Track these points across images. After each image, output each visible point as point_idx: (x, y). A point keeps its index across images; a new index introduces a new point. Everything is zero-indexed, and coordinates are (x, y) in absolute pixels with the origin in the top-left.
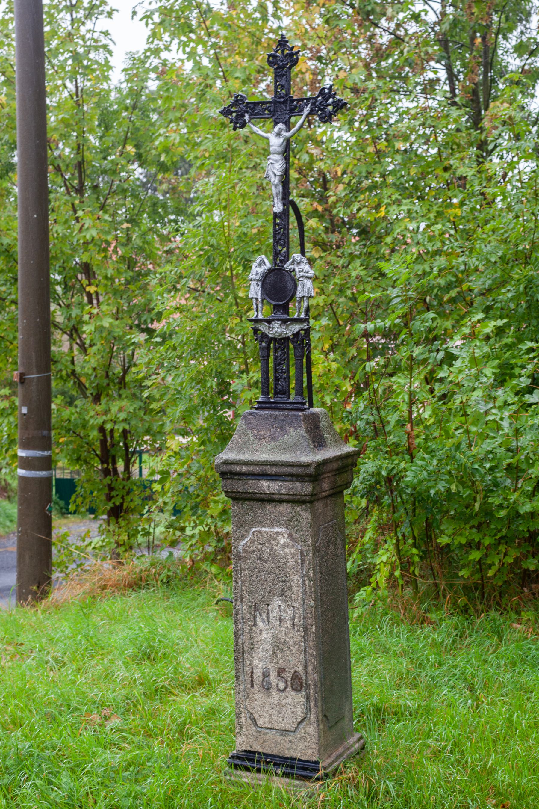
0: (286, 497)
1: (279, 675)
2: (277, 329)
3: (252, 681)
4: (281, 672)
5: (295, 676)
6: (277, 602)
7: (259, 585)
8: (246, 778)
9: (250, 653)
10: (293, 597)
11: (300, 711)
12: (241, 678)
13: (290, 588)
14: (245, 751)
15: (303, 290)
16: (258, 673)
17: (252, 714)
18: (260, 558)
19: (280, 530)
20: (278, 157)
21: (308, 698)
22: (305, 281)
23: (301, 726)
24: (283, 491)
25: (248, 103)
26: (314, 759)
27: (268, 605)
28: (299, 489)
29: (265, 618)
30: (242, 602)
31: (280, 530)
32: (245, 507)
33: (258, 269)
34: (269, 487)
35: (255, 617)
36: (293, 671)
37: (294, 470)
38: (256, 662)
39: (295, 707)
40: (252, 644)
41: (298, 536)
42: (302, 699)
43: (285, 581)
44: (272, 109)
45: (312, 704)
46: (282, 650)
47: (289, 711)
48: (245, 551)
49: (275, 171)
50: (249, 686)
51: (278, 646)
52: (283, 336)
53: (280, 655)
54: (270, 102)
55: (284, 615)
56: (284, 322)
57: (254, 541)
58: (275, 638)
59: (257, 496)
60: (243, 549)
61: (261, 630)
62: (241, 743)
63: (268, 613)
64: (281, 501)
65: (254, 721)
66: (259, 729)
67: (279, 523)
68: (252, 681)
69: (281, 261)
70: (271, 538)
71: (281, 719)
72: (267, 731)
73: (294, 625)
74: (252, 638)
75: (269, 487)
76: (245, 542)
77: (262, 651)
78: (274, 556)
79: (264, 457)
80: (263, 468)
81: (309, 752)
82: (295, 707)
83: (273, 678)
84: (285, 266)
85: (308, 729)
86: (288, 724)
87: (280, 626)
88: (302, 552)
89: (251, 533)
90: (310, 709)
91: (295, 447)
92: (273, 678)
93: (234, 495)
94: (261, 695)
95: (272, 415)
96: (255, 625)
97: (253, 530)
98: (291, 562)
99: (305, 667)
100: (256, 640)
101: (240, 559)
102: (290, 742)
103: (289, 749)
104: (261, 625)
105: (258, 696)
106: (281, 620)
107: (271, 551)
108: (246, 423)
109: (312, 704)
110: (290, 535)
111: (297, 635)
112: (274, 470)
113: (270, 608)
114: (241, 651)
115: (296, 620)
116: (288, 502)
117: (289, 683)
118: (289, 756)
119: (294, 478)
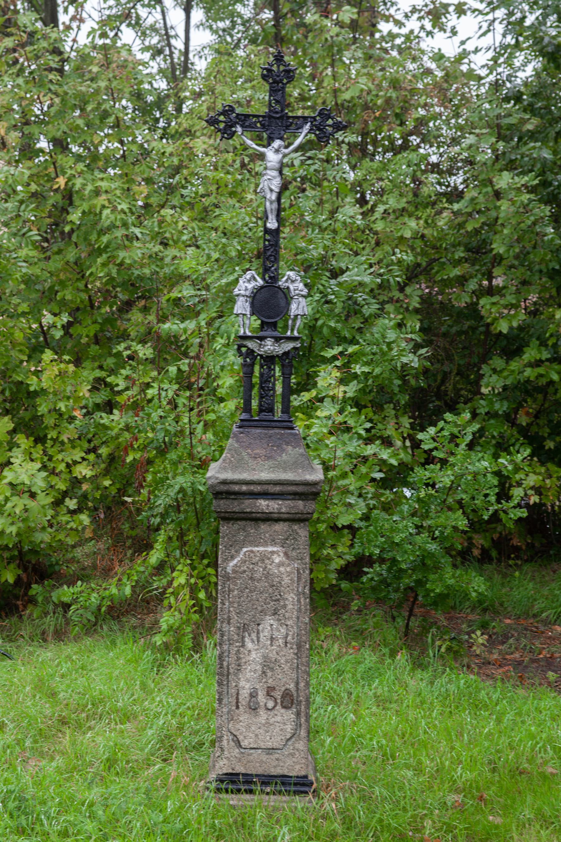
0: (286, 516)
1: (268, 694)
2: (269, 347)
3: (237, 702)
4: (269, 692)
5: (287, 694)
6: (269, 621)
7: (250, 605)
8: (233, 800)
9: (236, 675)
10: (287, 615)
11: (289, 728)
12: (225, 701)
13: (285, 606)
14: (226, 774)
15: (298, 308)
16: (245, 694)
17: (235, 736)
18: (251, 578)
19: (275, 549)
20: (275, 173)
21: (298, 714)
22: (301, 299)
23: (290, 743)
24: (284, 510)
25: (238, 114)
26: (303, 773)
27: (259, 625)
28: (301, 507)
29: (255, 639)
30: (229, 623)
31: (275, 549)
32: (236, 526)
33: (246, 284)
34: (268, 506)
35: (243, 637)
36: (283, 689)
37: (300, 489)
38: (242, 683)
39: (285, 724)
40: (239, 665)
41: (294, 554)
42: (293, 716)
43: (278, 600)
44: (267, 123)
45: (303, 720)
46: (272, 669)
47: (278, 729)
48: (234, 571)
49: (273, 187)
50: (234, 708)
51: (268, 665)
52: (274, 353)
53: (269, 674)
54: (263, 117)
55: (276, 634)
56: (277, 339)
57: (245, 561)
58: (266, 658)
59: (254, 515)
60: (233, 570)
61: (250, 651)
62: (223, 766)
63: (258, 633)
64: (277, 520)
65: (238, 743)
66: (242, 750)
67: (273, 542)
68: (237, 702)
69: (270, 278)
70: (264, 558)
71: (268, 738)
72: (252, 751)
73: (286, 643)
74: (239, 659)
75: (268, 506)
76: (235, 562)
77: (250, 671)
78: (268, 575)
79: (265, 476)
80: (265, 487)
81: (298, 767)
82: (285, 724)
83: (261, 697)
84: (280, 283)
85: (297, 745)
86: (276, 742)
87: (272, 645)
88: (298, 570)
89: (242, 553)
90: (301, 725)
91: (295, 465)
92: (261, 697)
93: (227, 515)
94: (247, 716)
95: (266, 434)
96: (243, 646)
97: (245, 550)
98: (286, 580)
99: (297, 684)
100: (244, 660)
101: (229, 580)
102: (277, 759)
103: (275, 767)
104: (249, 645)
105: (244, 717)
106: (272, 639)
107: (264, 570)
108: (237, 441)
109: (303, 720)
110: (286, 554)
111: (290, 653)
112: (278, 489)
113: (261, 627)
114: (225, 672)
115: (289, 638)
116: (285, 520)
117: (279, 701)
118: (275, 774)
119: (297, 497)
